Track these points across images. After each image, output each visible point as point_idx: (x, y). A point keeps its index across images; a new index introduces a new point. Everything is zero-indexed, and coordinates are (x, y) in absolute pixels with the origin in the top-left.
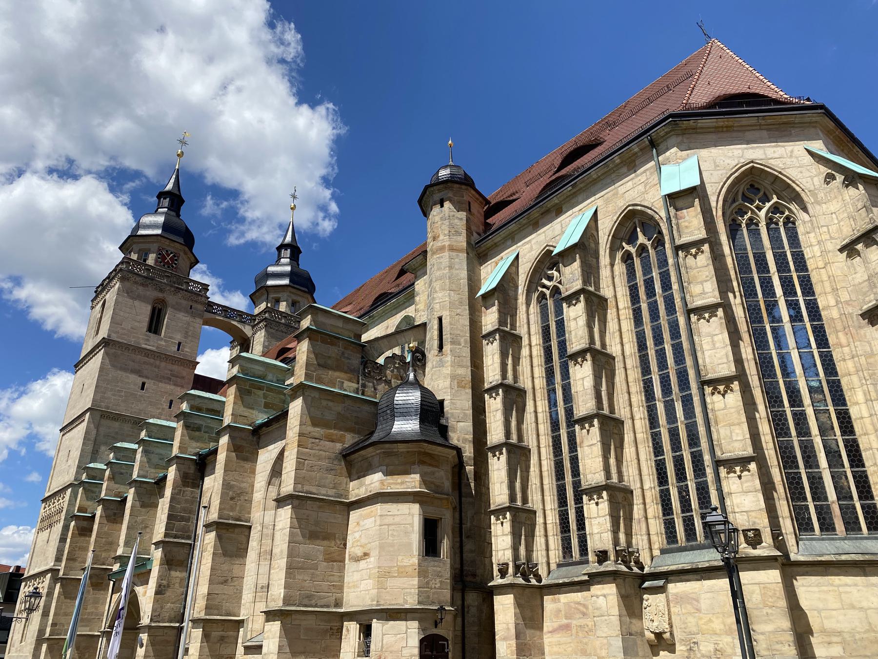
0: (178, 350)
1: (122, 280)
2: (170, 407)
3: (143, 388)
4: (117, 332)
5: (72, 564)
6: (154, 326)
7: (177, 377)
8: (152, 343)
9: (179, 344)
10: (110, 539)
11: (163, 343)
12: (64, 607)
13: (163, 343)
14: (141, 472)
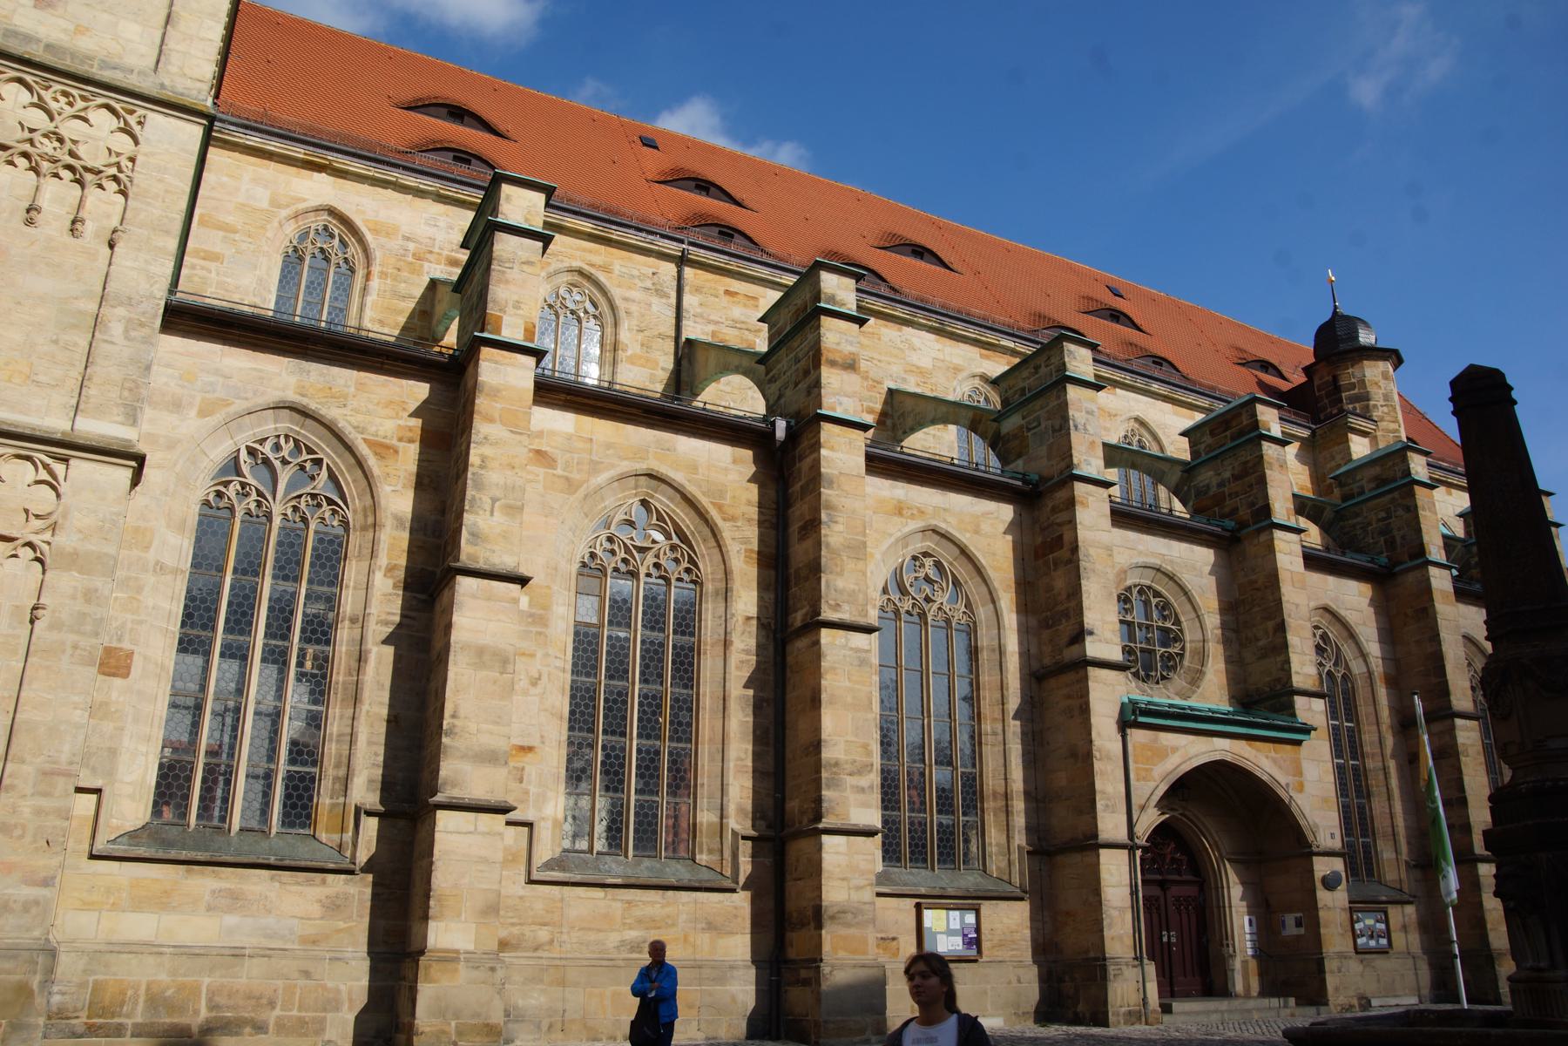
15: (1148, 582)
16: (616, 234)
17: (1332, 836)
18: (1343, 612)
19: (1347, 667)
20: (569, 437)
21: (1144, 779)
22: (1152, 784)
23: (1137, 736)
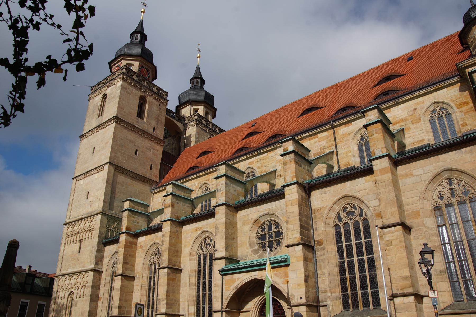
0: (154, 132)
1: (124, 80)
2: (151, 169)
3: (136, 154)
4: (121, 114)
5: (126, 266)
6: (140, 114)
7: (154, 149)
8: (141, 124)
9: (154, 127)
10: (177, 248)
11: (146, 126)
12: (124, 295)
13: (146, 126)
14: (227, 199)
15: (270, 219)
16: (208, 171)
17: (301, 298)
18: (354, 195)
19: (366, 215)
20: (144, 241)
21: (228, 290)
22: (230, 291)
23: (226, 277)
